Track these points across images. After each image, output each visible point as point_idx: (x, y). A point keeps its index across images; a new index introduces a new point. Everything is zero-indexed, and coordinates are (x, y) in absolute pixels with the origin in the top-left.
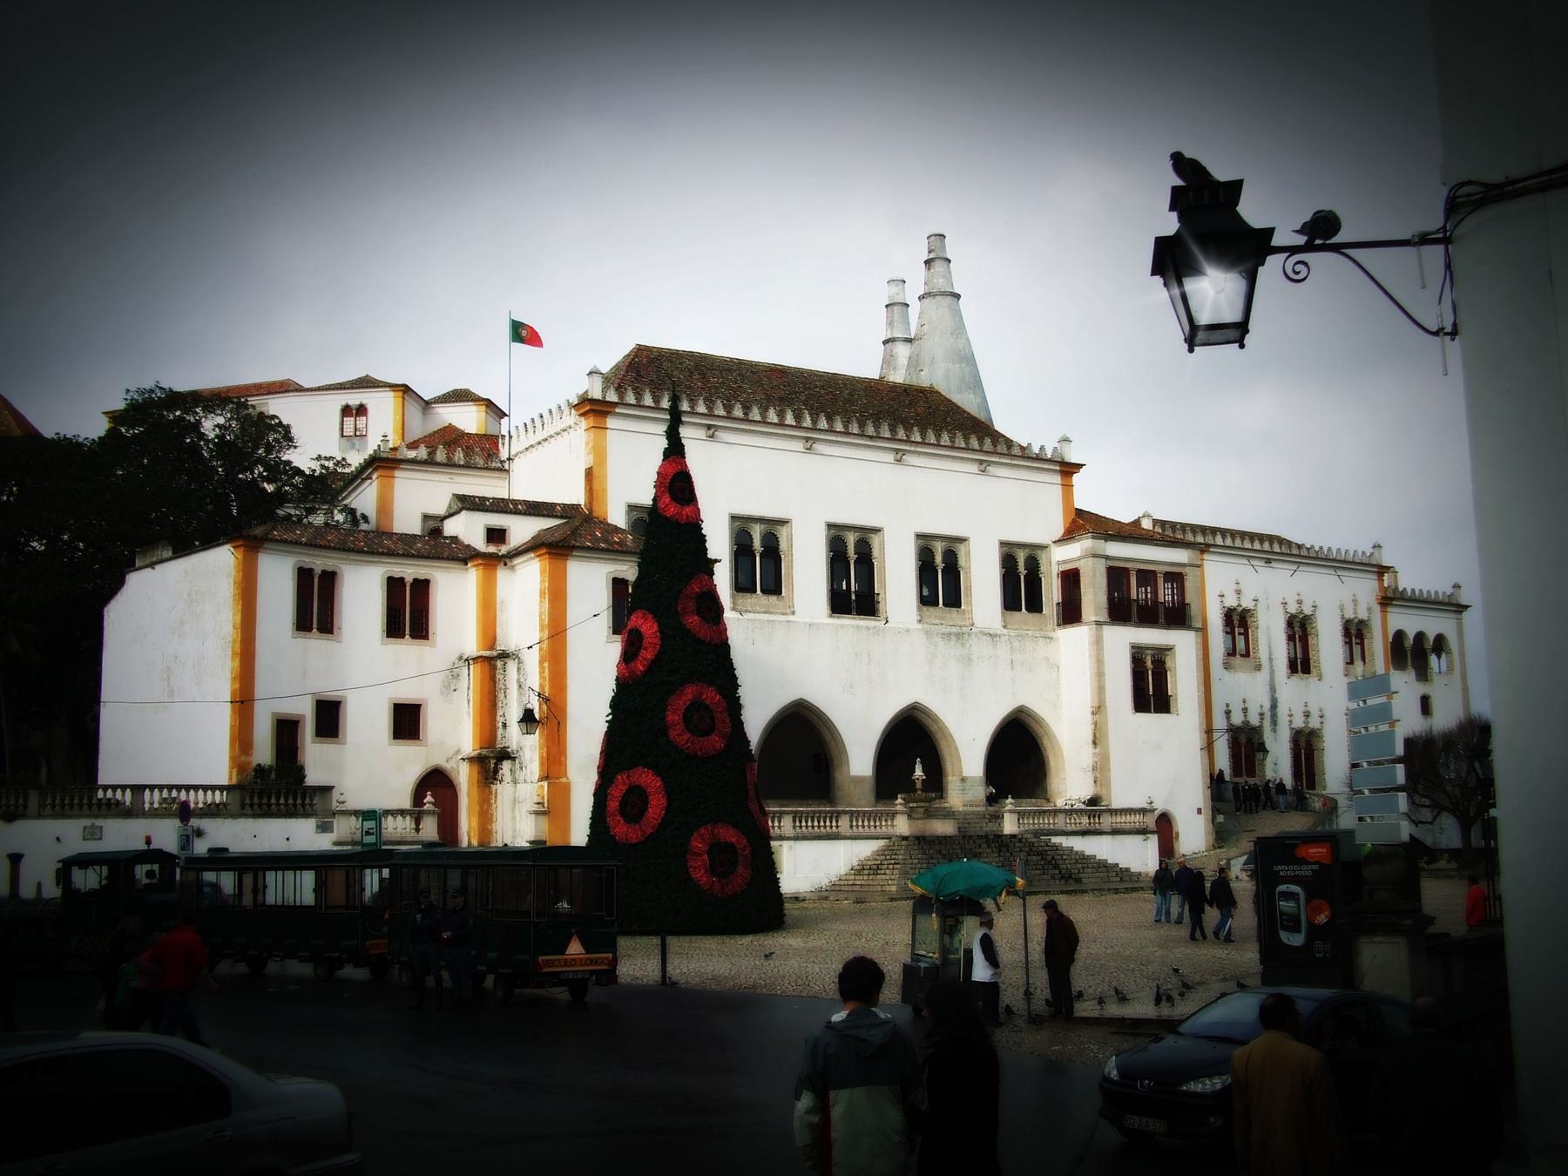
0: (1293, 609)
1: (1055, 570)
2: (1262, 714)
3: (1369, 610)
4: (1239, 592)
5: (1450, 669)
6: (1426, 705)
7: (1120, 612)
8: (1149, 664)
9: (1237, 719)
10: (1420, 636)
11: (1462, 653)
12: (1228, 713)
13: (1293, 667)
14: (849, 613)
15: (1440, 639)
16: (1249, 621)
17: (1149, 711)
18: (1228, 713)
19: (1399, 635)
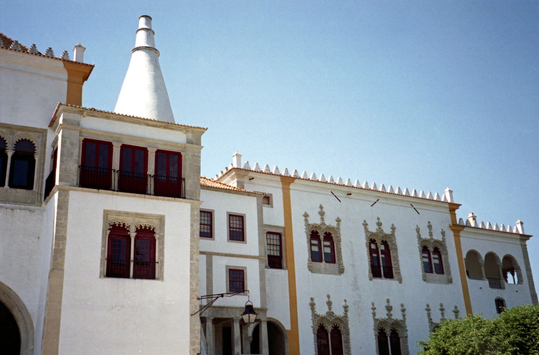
0: (373, 228)
1: (49, 151)
2: (346, 308)
3: (443, 233)
4: (322, 214)
5: (520, 281)
6: (500, 303)
8: (133, 235)
9: (322, 310)
10: (491, 256)
11: (529, 270)
12: (312, 305)
13: (375, 273)
15: (508, 259)
16: (333, 235)
17: (127, 276)
18: (312, 305)
19: (473, 255)
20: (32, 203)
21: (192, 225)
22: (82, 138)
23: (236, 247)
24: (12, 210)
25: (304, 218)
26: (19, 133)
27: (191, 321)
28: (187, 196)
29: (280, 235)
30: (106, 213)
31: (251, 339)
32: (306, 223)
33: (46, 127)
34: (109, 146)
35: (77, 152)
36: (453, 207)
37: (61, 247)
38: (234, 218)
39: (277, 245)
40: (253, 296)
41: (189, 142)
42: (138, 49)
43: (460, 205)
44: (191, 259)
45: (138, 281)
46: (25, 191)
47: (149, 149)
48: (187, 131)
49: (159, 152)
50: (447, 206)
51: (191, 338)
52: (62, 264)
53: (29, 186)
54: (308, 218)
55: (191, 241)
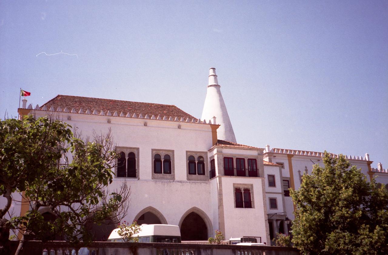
1: (209, 160)
4: (306, 170)
7: (228, 172)
8: (243, 192)
14: (126, 177)
17: (243, 207)
20: (205, 180)
21: (262, 187)
22: (223, 157)
23: (272, 189)
24: (201, 183)
25: (298, 173)
26: (198, 154)
27: (265, 223)
28: (260, 176)
29: (288, 181)
30: (234, 184)
31: (279, 227)
32: (299, 175)
33: (207, 151)
34: (232, 159)
35: (222, 162)
36: (369, 163)
37: (221, 197)
38: (270, 177)
39: (287, 186)
40: (280, 210)
41: (259, 154)
42: (211, 86)
43: (373, 162)
44: (263, 200)
45: (247, 209)
46: (203, 176)
47: (245, 159)
48: (258, 150)
49: (249, 159)
50: (366, 162)
51: (266, 229)
52: (222, 204)
53: (204, 174)
54: (300, 173)
55: (263, 193)
